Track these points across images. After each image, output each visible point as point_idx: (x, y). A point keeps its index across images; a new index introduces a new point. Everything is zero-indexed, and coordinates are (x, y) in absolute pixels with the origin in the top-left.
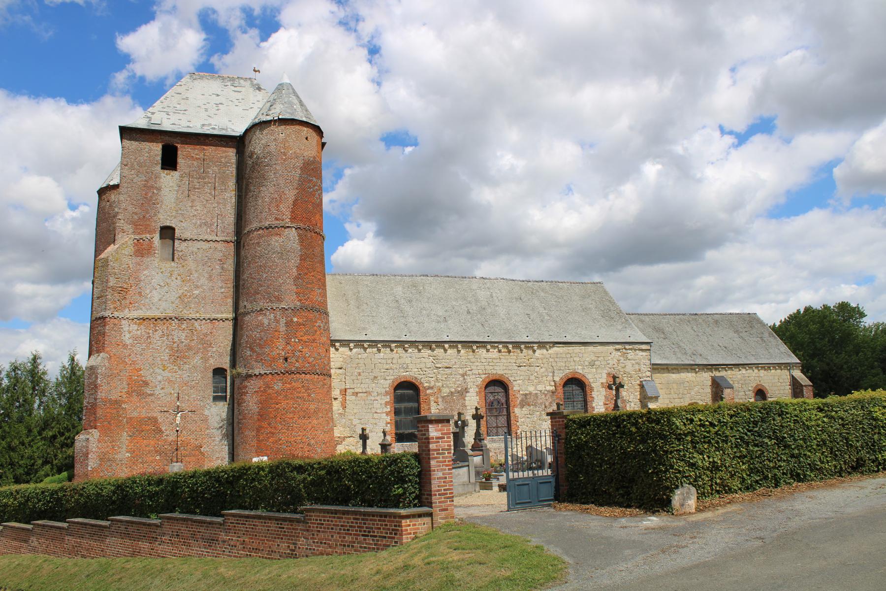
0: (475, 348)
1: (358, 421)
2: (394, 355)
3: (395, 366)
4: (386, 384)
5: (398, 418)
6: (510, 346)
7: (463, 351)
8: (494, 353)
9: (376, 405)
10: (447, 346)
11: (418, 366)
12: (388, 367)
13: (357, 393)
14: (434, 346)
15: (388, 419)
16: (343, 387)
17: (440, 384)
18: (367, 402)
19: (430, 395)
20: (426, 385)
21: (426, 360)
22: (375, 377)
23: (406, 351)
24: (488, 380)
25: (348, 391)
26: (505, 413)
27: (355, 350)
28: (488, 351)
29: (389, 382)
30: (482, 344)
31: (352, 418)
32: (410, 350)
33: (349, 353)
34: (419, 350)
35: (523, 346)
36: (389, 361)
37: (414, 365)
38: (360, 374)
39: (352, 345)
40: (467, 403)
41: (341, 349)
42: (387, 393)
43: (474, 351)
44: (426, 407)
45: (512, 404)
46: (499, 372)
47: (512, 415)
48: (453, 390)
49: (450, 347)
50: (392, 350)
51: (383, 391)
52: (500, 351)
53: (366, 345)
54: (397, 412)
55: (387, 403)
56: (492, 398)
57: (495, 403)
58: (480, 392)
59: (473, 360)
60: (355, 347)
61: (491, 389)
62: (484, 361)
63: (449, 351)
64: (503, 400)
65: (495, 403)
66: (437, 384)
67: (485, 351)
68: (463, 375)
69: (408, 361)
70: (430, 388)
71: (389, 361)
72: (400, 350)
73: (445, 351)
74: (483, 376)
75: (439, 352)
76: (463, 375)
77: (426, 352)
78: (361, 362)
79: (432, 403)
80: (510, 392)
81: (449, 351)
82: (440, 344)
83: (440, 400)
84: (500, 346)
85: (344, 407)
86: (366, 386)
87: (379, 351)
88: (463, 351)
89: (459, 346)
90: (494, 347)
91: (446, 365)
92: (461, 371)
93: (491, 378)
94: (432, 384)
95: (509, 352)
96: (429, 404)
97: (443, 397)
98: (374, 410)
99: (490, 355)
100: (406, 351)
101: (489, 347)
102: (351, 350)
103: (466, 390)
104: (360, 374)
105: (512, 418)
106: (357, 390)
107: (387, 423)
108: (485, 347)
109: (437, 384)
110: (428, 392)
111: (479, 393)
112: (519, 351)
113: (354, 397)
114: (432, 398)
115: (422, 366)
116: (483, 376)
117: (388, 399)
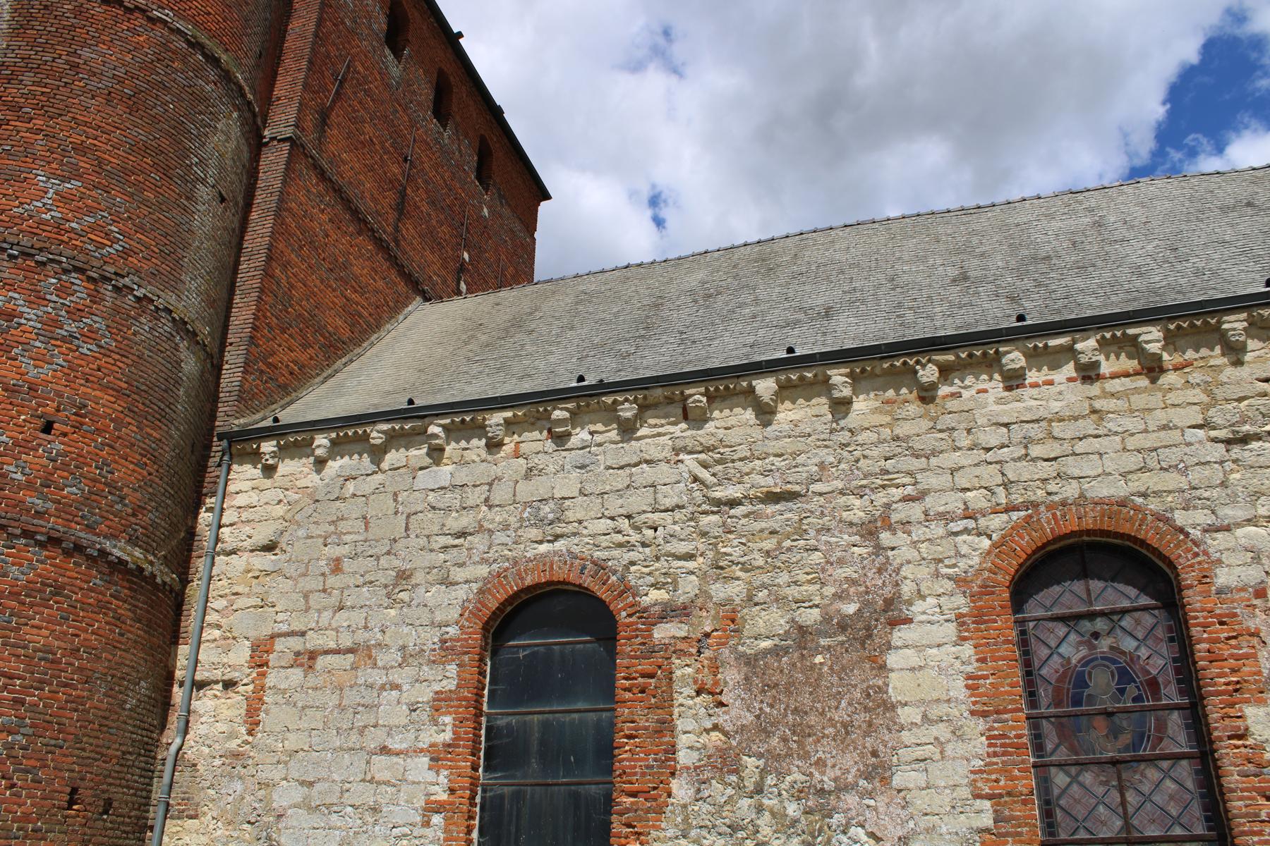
0: (928, 373)
1: (298, 794)
2: (506, 465)
3: (498, 516)
4: (447, 608)
5: (504, 786)
6: (1152, 337)
7: (862, 405)
8: (1054, 390)
9: (392, 710)
10: (765, 386)
11: (614, 505)
12: (466, 521)
13: (313, 655)
14: (696, 396)
15: (439, 786)
16: (266, 631)
17: (735, 590)
18: (351, 697)
19: (673, 649)
20: (655, 595)
21: (663, 472)
22: (403, 576)
23: (560, 439)
24: (1026, 543)
25: (280, 644)
26: (1178, 737)
27: (334, 466)
28: (1014, 380)
29: (461, 593)
30: (974, 349)
31: (276, 774)
32: (581, 435)
33: (313, 479)
34: (628, 430)
35: (1235, 324)
36: (475, 497)
37: (591, 502)
38: (337, 566)
39: (322, 441)
40: (898, 686)
41: (286, 467)
42: (446, 649)
43: (927, 395)
44: (647, 721)
45: (1216, 678)
46: (1102, 490)
47: (1228, 753)
48: (811, 616)
49: (786, 391)
50: (494, 445)
51: (431, 638)
52: (1089, 373)
53: (376, 434)
54: (499, 751)
55: (440, 702)
56: (1072, 651)
57: (1101, 683)
58: (979, 617)
59: (931, 440)
60: (337, 447)
61: (1066, 595)
62: (992, 437)
63: (787, 414)
64: (1156, 660)
65: (1101, 683)
66: (719, 591)
67: (995, 386)
68: (869, 531)
69: (567, 485)
70: (669, 612)
71: (475, 497)
72: (534, 441)
73: (765, 413)
74: (997, 522)
75: (730, 424)
76: (869, 531)
77: (659, 436)
78: (352, 509)
79: (684, 695)
80: (1194, 599)
81: (787, 414)
82: (728, 382)
83: (731, 676)
84: (1087, 345)
85: (252, 721)
86: (357, 617)
87: (436, 453)
88: (862, 405)
89: (838, 376)
90: (1054, 359)
91: (769, 483)
92: (858, 509)
93: (1048, 527)
94: (689, 587)
95: (1153, 369)
96: (666, 703)
97: (750, 661)
98: (374, 739)
99: (1027, 402)
100: (560, 439)
101: (1014, 358)
102: (320, 463)
103: (893, 613)
104: (337, 566)
105: (1232, 778)
106: (315, 641)
107: (433, 808)
108: (992, 364)
109: (719, 591)
110: (662, 632)
111: (971, 624)
112: (1216, 357)
113: (296, 674)
114: (684, 670)
115: (637, 501)
116: (997, 522)
117: (448, 678)
